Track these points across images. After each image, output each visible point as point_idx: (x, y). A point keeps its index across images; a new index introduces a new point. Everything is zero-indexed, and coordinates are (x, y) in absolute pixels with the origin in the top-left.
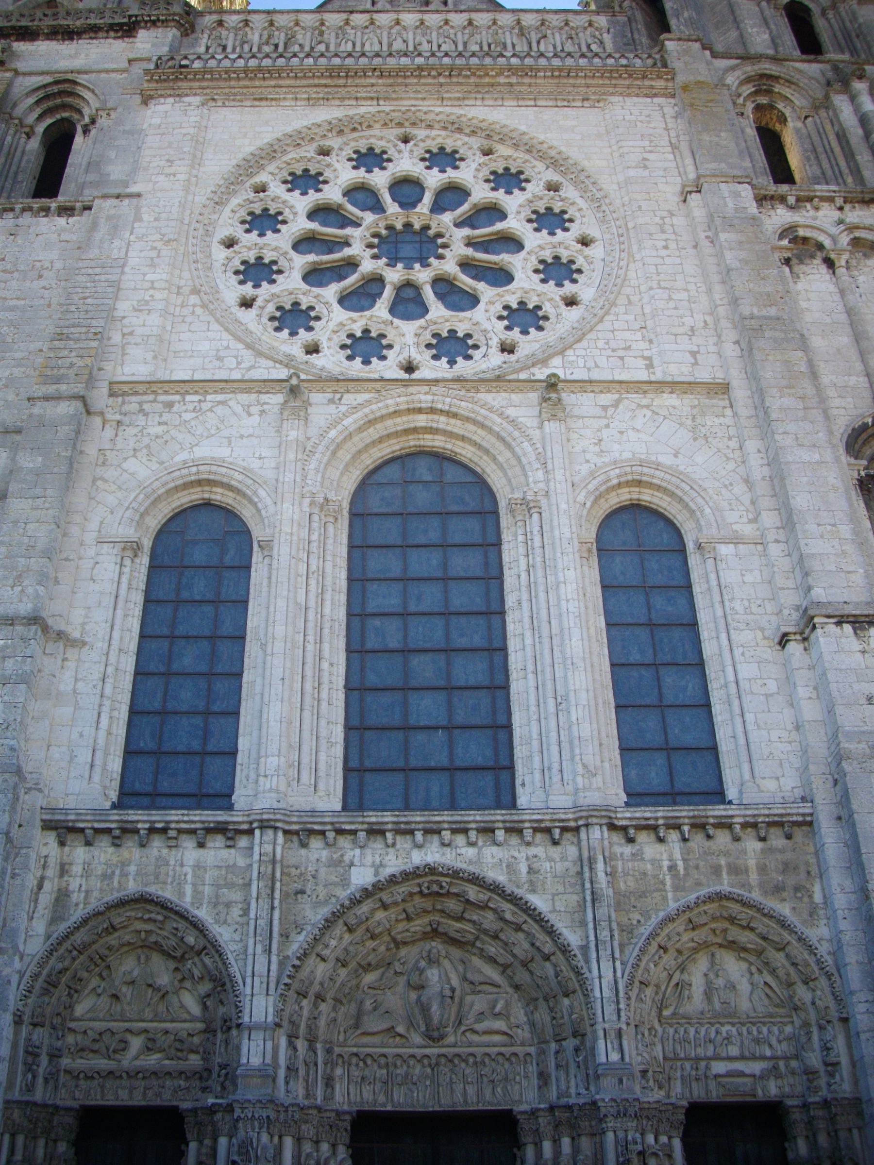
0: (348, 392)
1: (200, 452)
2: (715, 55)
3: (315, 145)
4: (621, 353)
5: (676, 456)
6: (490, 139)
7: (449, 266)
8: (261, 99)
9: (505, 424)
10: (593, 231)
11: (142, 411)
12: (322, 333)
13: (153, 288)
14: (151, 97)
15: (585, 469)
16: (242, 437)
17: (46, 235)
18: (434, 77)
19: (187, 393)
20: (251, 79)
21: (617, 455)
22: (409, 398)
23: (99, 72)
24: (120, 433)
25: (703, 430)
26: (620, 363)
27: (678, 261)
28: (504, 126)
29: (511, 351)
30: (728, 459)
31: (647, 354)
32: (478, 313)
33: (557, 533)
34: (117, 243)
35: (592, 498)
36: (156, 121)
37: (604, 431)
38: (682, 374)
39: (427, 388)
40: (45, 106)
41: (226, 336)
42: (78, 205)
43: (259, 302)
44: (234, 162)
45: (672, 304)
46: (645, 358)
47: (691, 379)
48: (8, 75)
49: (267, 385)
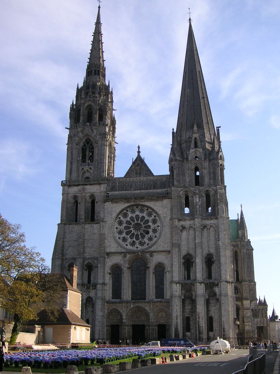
7: (142, 232)
10: (159, 225)
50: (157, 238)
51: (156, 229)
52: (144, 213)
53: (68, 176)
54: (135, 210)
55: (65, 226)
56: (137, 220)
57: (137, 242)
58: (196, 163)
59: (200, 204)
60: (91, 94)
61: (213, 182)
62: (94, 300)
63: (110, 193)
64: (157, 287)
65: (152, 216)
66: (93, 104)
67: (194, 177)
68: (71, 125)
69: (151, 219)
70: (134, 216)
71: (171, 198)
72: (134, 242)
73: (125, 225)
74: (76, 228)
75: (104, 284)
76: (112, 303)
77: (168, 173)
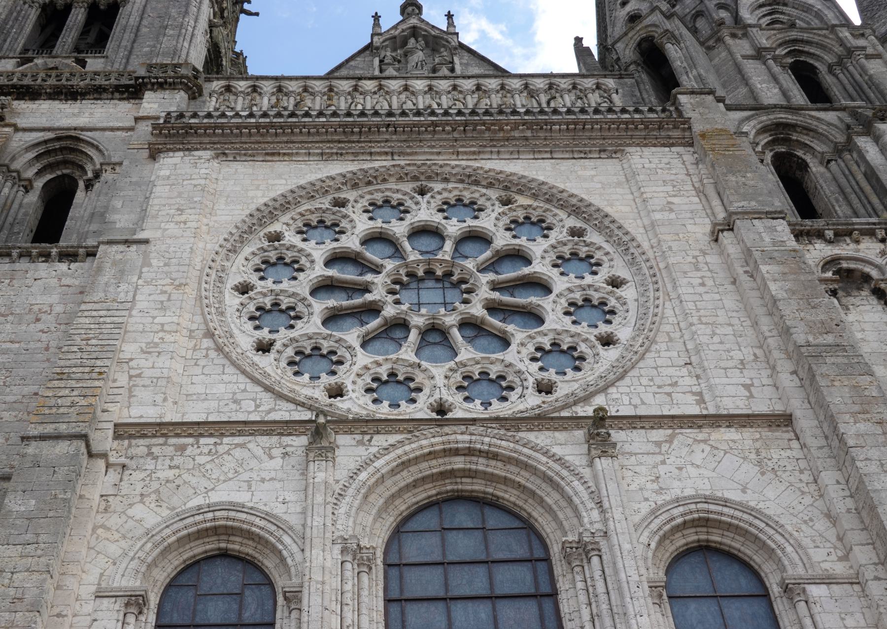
0: (378, 433)
1: (215, 497)
2: (729, 108)
3: (330, 198)
4: (668, 389)
5: (744, 491)
6: (509, 188)
7: (477, 310)
8: (273, 154)
9: (551, 463)
10: (622, 272)
11: (150, 454)
12: (346, 376)
13: (163, 330)
14: (160, 151)
15: (645, 508)
16: (263, 480)
17: (45, 283)
18: (449, 133)
19: (201, 435)
20: (262, 135)
21: (679, 492)
22: (445, 438)
23: (104, 129)
24: (125, 478)
25: (769, 463)
26: (668, 399)
27: (717, 297)
28: (523, 177)
29: (549, 392)
30: (803, 493)
31: (695, 389)
32: (510, 355)
33: (623, 576)
34: (123, 287)
35: (657, 538)
36: (165, 172)
37: (660, 467)
38: (738, 407)
39: (463, 428)
40: (45, 162)
41: (242, 378)
42: (81, 251)
43: (278, 346)
45: (716, 339)
46: (694, 394)
47: (750, 412)
49: (287, 427)
58: (795, 41)
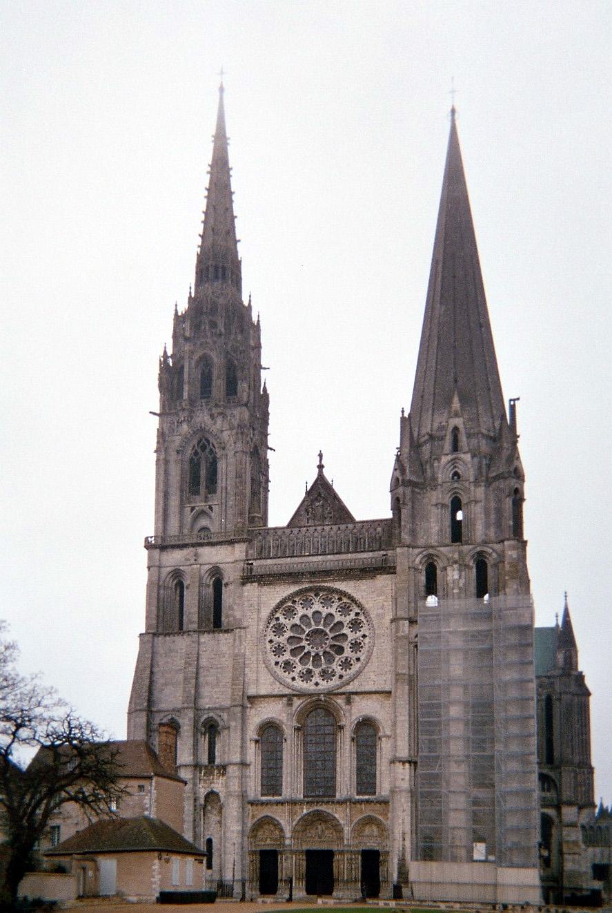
7: (328, 650)
34: (243, 647)
44: (269, 611)
48: (198, 566)
50: (362, 664)
51: (360, 643)
52: (331, 606)
53: (160, 526)
54: (311, 600)
55: (156, 639)
56: (317, 623)
57: (317, 671)
59: (461, 585)
60: (207, 328)
61: (496, 533)
62: (222, 799)
63: (255, 563)
64: (360, 770)
65: (351, 613)
66: (213, 355)
67: (448, 522)
68: (163, 406)
69: (347, 620)
70: (309, 613)
71: (395, 573)
72: (309, 671)
73: (288, 634)
74: (182, 644)
75: (244, 764)
76: (263, 803)
77: (388, 514)
